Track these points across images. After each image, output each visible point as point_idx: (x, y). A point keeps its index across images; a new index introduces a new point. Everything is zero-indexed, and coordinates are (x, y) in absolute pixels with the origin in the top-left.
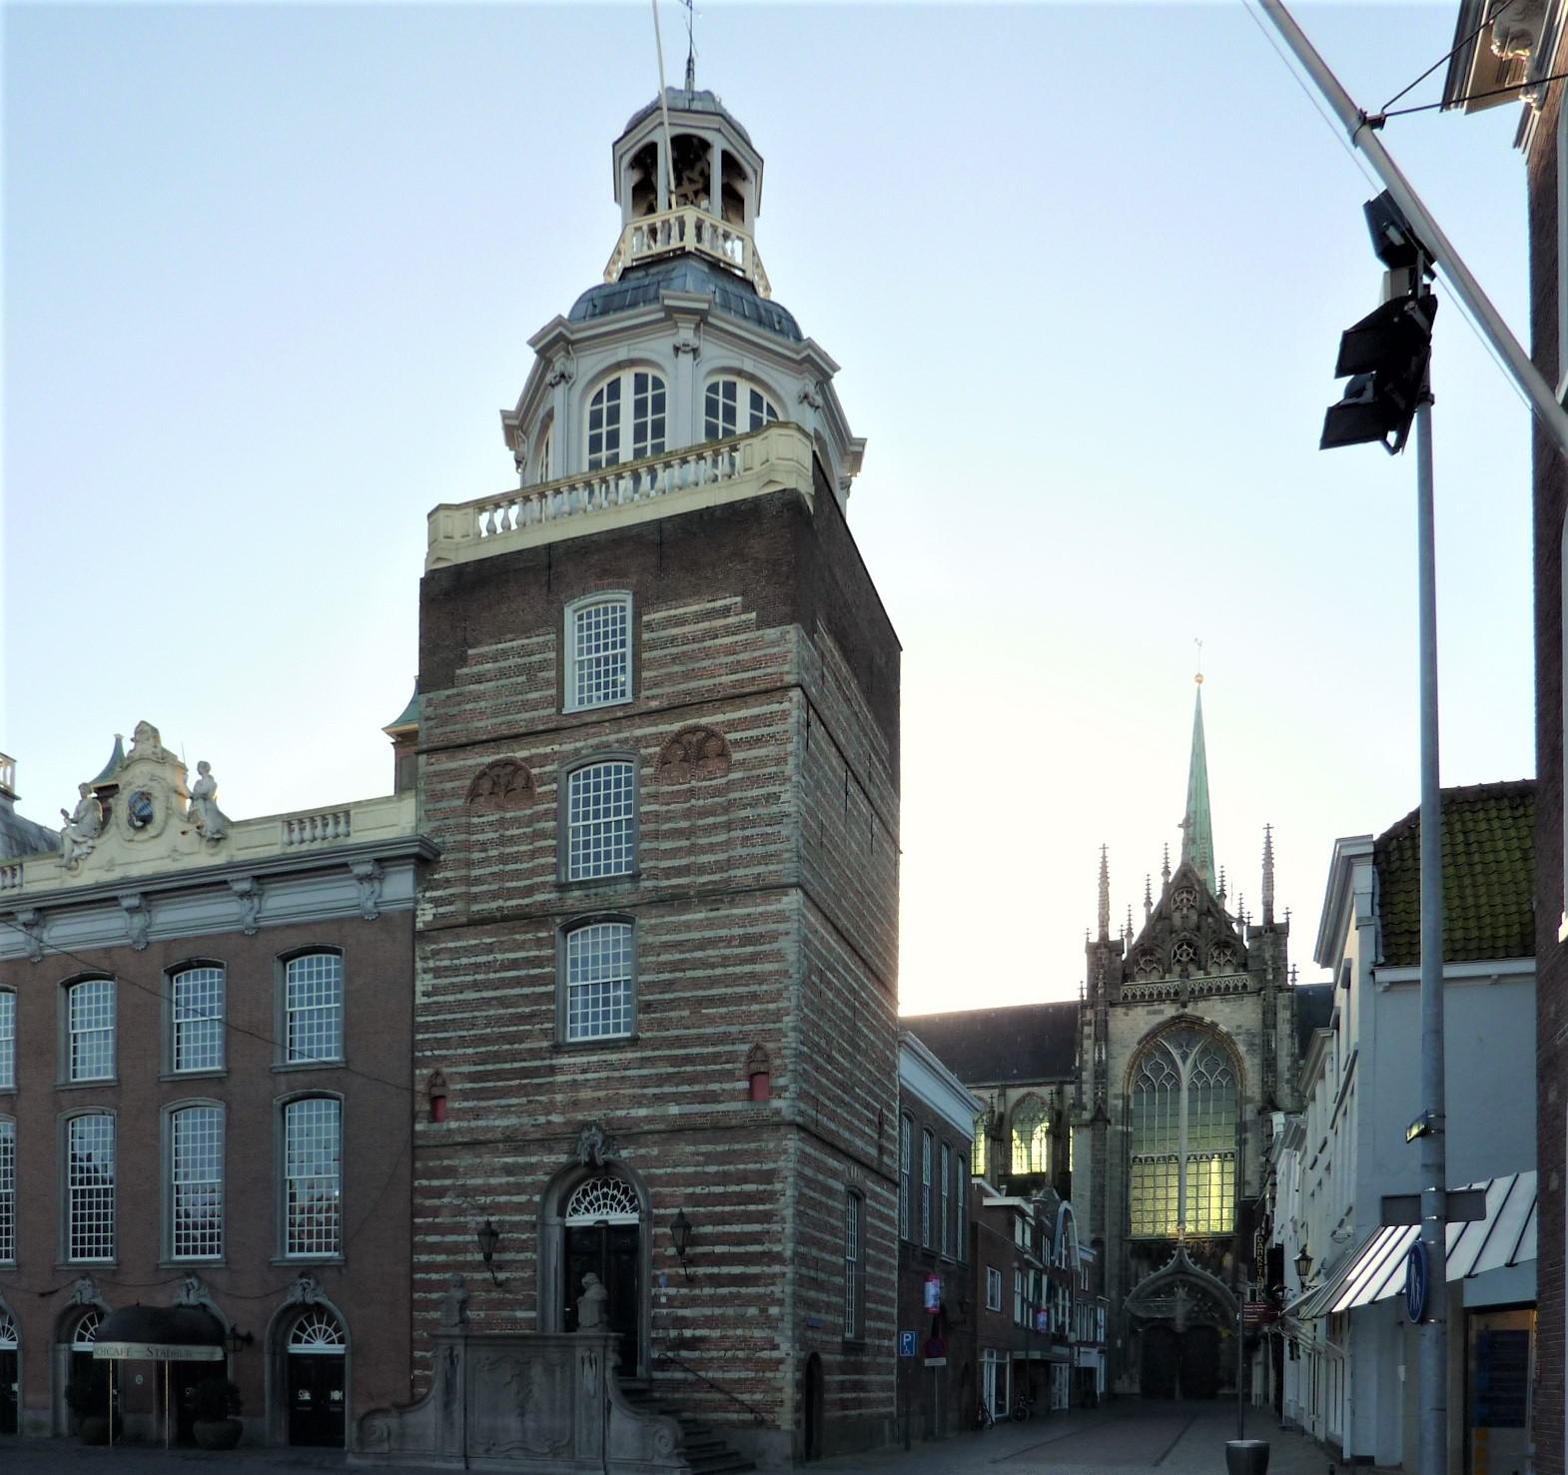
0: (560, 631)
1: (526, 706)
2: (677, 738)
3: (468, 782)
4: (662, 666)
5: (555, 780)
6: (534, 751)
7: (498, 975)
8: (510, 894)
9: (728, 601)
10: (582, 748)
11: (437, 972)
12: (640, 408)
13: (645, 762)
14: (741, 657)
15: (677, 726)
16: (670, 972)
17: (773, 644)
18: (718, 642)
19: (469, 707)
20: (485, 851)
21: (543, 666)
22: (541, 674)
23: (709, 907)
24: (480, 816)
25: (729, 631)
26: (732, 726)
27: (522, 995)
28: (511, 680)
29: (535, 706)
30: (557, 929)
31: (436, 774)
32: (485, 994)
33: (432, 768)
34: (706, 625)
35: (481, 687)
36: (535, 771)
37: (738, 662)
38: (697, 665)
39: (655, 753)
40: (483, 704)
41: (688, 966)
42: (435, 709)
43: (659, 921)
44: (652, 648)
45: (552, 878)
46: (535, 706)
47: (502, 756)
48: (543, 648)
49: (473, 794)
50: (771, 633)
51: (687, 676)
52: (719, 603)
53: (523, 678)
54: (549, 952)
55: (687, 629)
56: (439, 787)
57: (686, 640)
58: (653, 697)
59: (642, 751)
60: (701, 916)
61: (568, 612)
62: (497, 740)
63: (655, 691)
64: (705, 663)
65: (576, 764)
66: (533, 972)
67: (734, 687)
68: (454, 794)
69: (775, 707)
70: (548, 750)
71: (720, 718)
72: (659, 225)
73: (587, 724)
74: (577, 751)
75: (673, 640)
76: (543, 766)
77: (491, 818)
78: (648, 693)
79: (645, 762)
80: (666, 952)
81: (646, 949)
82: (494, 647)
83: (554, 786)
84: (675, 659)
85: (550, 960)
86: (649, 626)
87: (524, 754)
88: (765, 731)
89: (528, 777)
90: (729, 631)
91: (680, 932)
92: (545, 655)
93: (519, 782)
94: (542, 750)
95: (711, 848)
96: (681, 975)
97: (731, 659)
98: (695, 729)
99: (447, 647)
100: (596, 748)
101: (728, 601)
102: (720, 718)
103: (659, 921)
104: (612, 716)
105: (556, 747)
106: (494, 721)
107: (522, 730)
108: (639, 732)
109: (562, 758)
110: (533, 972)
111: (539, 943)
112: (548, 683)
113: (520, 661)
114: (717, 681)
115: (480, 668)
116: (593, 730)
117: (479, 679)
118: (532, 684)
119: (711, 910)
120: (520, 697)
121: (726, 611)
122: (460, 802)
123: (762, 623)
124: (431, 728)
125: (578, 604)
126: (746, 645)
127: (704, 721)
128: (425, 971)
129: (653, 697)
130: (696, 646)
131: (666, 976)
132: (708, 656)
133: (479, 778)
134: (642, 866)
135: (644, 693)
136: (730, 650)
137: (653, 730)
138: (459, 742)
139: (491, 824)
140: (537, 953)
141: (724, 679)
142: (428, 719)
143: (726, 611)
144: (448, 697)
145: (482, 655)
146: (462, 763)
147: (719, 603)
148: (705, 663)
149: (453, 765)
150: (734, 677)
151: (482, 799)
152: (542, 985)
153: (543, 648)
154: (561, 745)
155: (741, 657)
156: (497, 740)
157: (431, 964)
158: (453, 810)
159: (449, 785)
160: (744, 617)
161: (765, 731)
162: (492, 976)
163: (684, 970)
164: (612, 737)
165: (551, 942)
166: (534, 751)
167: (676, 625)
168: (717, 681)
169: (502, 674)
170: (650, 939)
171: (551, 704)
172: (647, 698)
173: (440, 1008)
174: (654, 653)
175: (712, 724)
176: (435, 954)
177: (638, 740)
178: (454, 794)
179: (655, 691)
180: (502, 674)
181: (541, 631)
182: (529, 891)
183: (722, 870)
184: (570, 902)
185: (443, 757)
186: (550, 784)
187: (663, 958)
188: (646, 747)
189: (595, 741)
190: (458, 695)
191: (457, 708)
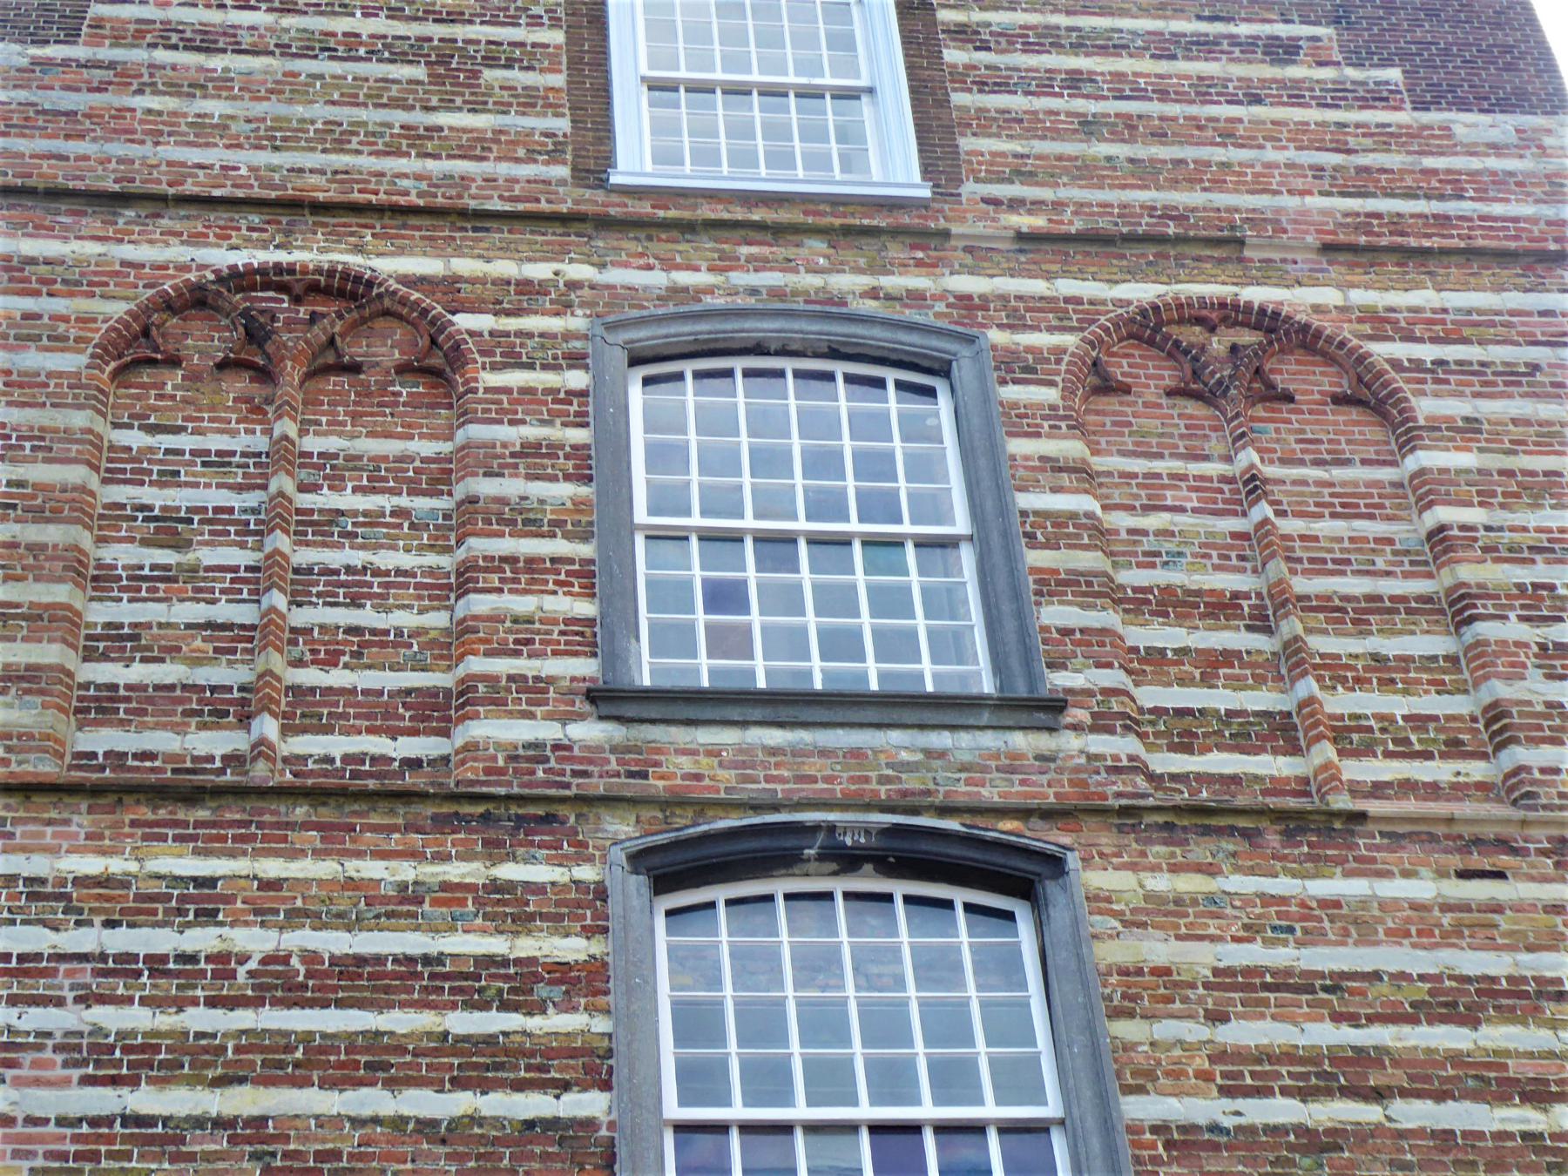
2: (1147, 328)
5: (576, 360)
7: (244, 1019)
8: (307, 710)
10: (710, 290)
15: (1142, 292)
16: (1305, 1094)
20: (182, 545)
23: (1456, 861)
27: (399, 1122)
30: (619, 855)
32: (145, 1100)
39: (1059, 351)
41: (1399, 1077)
43: (1190, 884)
45: (585, 667)
53: (419, 72)
54: (572, 948)
55: (1125, 64)
60: (1423, 888)
66: (462, 1022)
77: (216, 442)
80: (1255, 1010)
81: (1153, 989)
85: (583, 982)
89: (436, 334)
91: (1312, 938)
93: (385, 349)
96: (1369, 1113)
98: (1232, 314)
103: (1190, 884)
109: (612, 308)
110: (462, 1022)
111: (508, 907)
113: (400, 28)
119: (1464, 875)
131: (1281, 1110)
134: (1061, 680)
140: (496, 945)
151: (173, 380)
152: (519, 1086)
162: (199, 1019)
163: (1379, 1095)
165: (587, 908)
170: (1157, 949)
177: (965, 300)
182: (435, 712)
183: (1454, 749)
184: (686, 764)
187: (1245, 1033)
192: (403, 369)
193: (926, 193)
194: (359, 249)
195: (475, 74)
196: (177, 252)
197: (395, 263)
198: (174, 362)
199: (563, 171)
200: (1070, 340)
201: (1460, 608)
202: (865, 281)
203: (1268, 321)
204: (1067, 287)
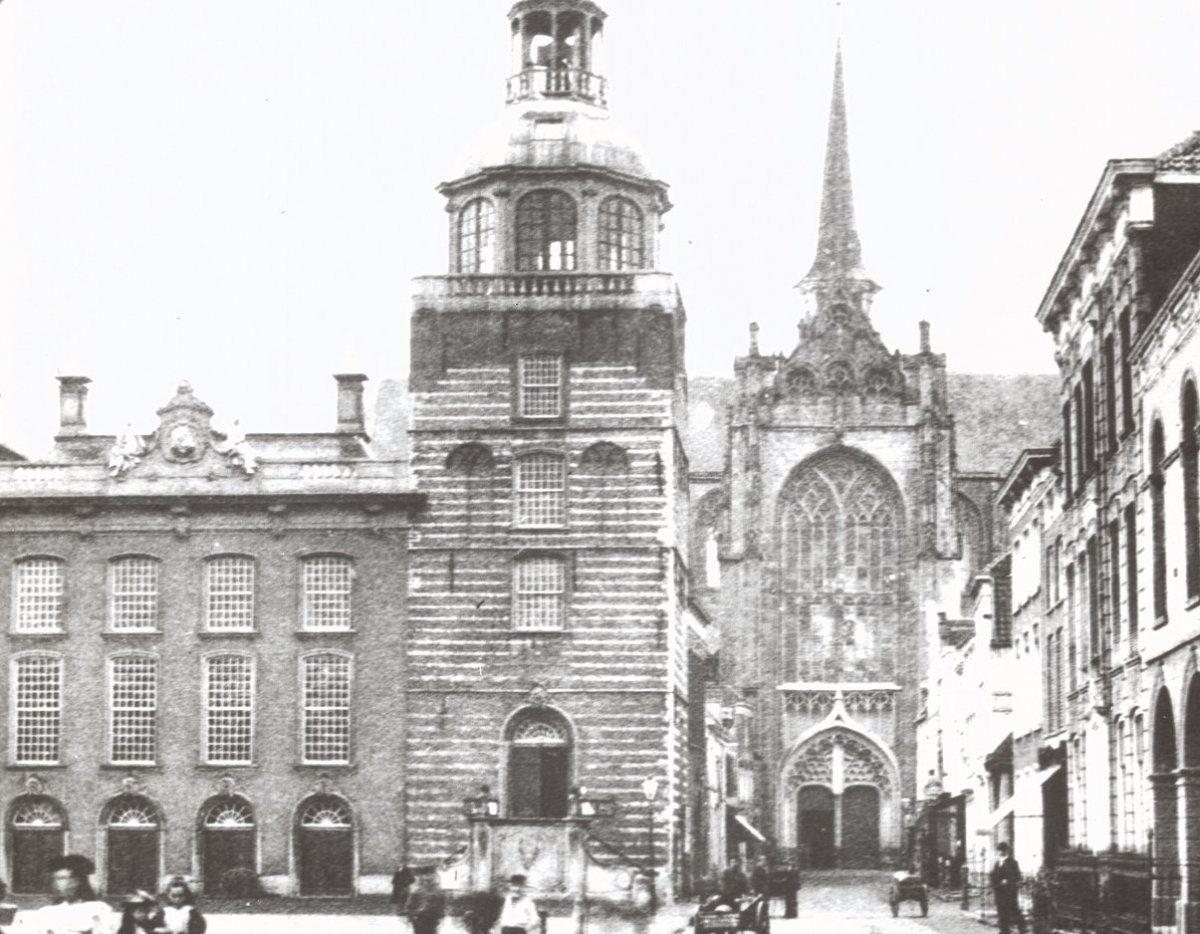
0: (514, 369)
2: (594, 448)
11: (424, 577)
13: (574, 459)
21: (500, 387)
29: (495, 412)
49: (448, 462)
50: (656, 393)
65: (526, 456)
79: (574, 459)
95: (617, 517)
98: (610, 444)
112: (503, 399)
123: (653, 385)
128: (416, 575)
139: (460, 483)
143: (626, 374)
157: (419, 571)
173: (426, 601)
176: (422, 565)
197: (486, 441)
201: (628, 506)
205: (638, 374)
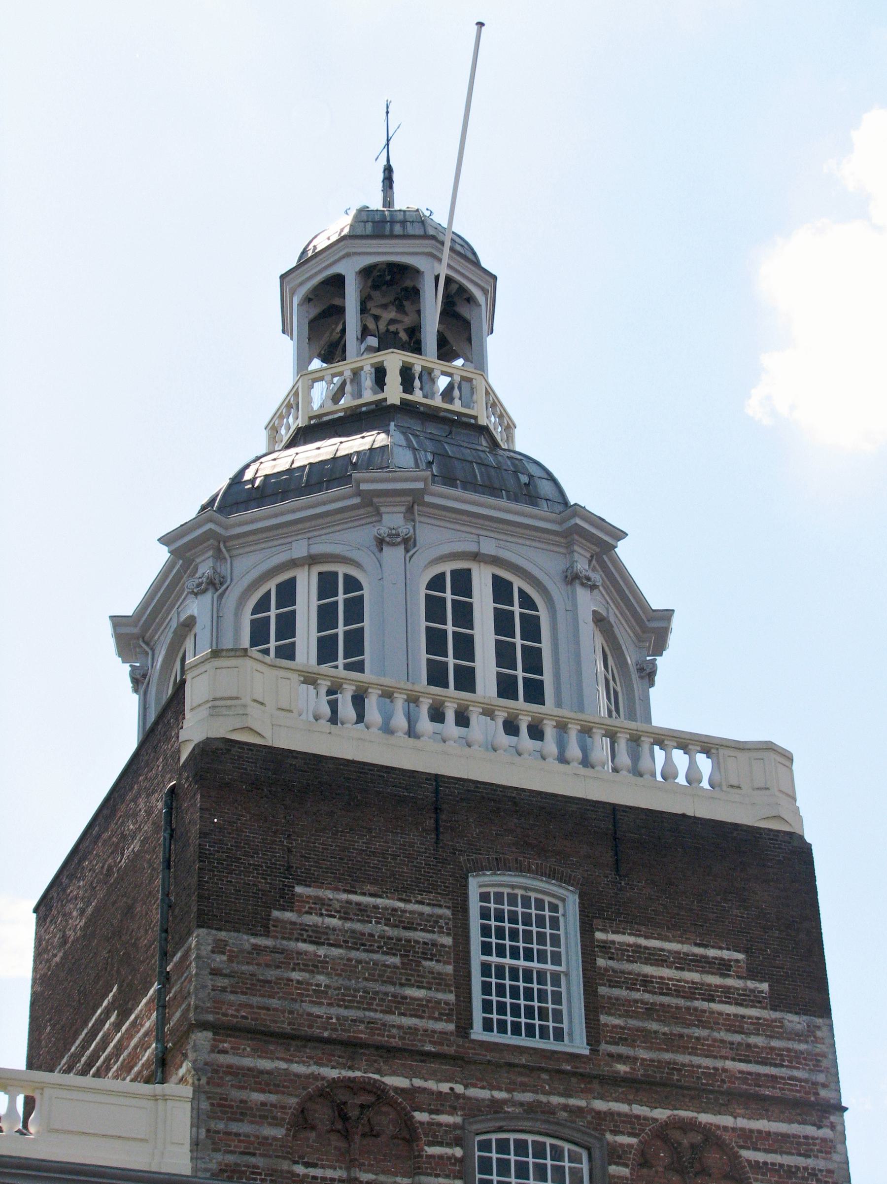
0: (461, 909)
1: (400, 1004)
3: (293, 1101)
4: (635, 1015)
5: (458, 1142)
6: (418, 1082)
9: (726, 954)
12: (503, 622)
14: (752, 1040)
15: (661, 1114)
17: (798, 1036)
18: (716, 1007)
19: (296, 975)
21: (431, 951)
22: (427, 964)
24: (307, 1165)
25: (728, 995)
26: (750, 1139)
28: (376, 957)
29: (419, 1009)
31: (232, 1071)
33: (222, 1059)
34: (695, 976)
35: (322, 951)
36: (421, 1116)
37: (748, 1046)
38: (686, 1031)
39: (630, 1146)
40: (321, 979)
42: (231, 960)
44: (613, 984)
46: (419, 1009)
47: (358, 1074)
48: (432, 924)
49: (302, 1121)
51: (672, 1043)
52: (712, 953)
53: (396, 960)
55: (666, 972)
56: (237, 1094)
57: (664, 987)
58: (620, 1058)
59: (609, 1137)
61: (475, 886)
62: (350, 1048)
63: (622, 1049)
64: (697, 1032)
67: (744, 1080)
68: (264, 1114)
69: (810, 1130)
70: (445, 1087)
71: (727, 1121)
72: (417, 369)
73: (510, 1065)
74: (495, 1106)
75: (646, 982)
76: (437, 1112)
78: (612, 1049)
79: (616, 1155)
82: (344, 896)
83: (458, 1152)
84: (651, 1011)
86: (606, 948)
87: (401, 1082)
88: (801, 1161)
89: (408, 1124)
90: (728, 995)
92: (435, 936)
94: (431, 1085)
97: (737, 1038)
99: (256, 867)
100: (531, 1109)
101: (726, 954)
102: (727, 1121)
104: (552, 1065)
105: (459, 1089)
106: (343, 1012)
107: (395, 1042)
108: (600, 1105)
112: (439, 982)
113: (390, 932)
114: (719, 1064)
115: (312, 919)
116: (520, 1079)
117: (317, 936)
118: (411, 972)
120: (391, 989)
121: (723, 967)
122: (279, 1132)
123: (776, 1002)
124: (224, 990)
125: (488, 878)
126: (759, 1027)
127: (705, 1118)
129: (620, 1058)
130: (681, 1002)
132: (702, 1024)
133: (310, 1098)
135: (604, 1047)
136: (735, 1024)
137: (624, 1108)
138: (274, 1027)
141: (729, 1064)
142: (215, 972)
143: (723, 967)
144: (256, 947)
145: (320, 901)
146: (283, 1065)
147: (712, 953)
148: (697, 1032)
149: (265, 1064)
150: (743, 1066)
151: (313, 1135)
153: (432, 924)
154: (466, 1087)
155: (752, 1040)
156: (350, 1048)
158: (265, 1141)
159: (257, 1097)
160: (751, 984)
161: (801, 1161)
164: (555, 1100)
166: (418, 1082)
167: (647, 961)
168: (719, 1064)
169: (358, 941)
171: (447, 1016)
172: (611, 1055)
174: (616, 992)
175: (718, 1127)
178: (264, 1114)
179: (622, 1049)
180: (358, 941)
181: (424, 897)
185: (247, 1046)
186: (449, 1145)
188: (615, 1133)
189: (528, 1097)
190: (274, 950)
191: (278, 972)
192: (394, 1137)
193: (586, 1052)
194: (378, 1071)
195: (419, 964)
196: (314, 1069)
198: (313, 1128)
199: (451, 1027)
200: (634, 1141)
202: (562, 1100)
203: (707, 1131)
204: (639, 1110)
205: (753, 974)
